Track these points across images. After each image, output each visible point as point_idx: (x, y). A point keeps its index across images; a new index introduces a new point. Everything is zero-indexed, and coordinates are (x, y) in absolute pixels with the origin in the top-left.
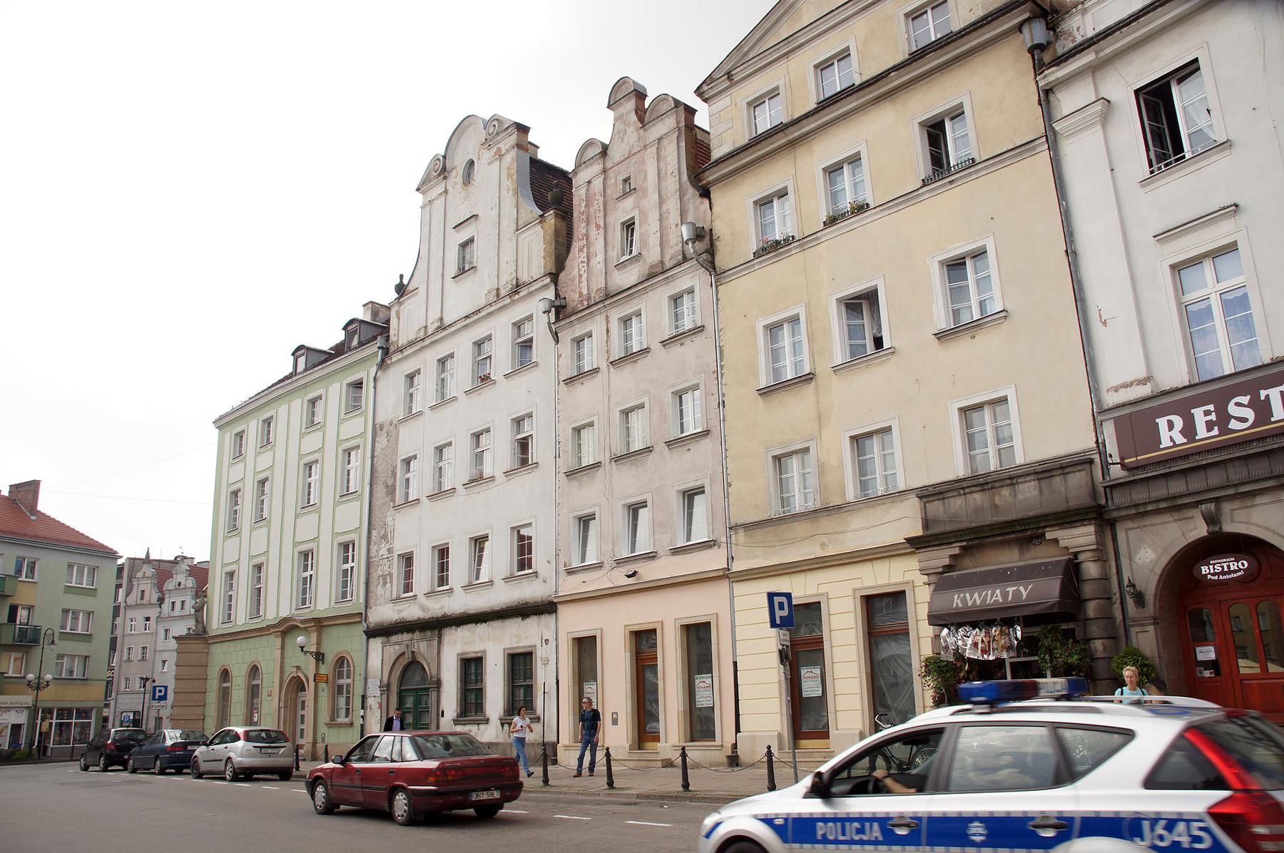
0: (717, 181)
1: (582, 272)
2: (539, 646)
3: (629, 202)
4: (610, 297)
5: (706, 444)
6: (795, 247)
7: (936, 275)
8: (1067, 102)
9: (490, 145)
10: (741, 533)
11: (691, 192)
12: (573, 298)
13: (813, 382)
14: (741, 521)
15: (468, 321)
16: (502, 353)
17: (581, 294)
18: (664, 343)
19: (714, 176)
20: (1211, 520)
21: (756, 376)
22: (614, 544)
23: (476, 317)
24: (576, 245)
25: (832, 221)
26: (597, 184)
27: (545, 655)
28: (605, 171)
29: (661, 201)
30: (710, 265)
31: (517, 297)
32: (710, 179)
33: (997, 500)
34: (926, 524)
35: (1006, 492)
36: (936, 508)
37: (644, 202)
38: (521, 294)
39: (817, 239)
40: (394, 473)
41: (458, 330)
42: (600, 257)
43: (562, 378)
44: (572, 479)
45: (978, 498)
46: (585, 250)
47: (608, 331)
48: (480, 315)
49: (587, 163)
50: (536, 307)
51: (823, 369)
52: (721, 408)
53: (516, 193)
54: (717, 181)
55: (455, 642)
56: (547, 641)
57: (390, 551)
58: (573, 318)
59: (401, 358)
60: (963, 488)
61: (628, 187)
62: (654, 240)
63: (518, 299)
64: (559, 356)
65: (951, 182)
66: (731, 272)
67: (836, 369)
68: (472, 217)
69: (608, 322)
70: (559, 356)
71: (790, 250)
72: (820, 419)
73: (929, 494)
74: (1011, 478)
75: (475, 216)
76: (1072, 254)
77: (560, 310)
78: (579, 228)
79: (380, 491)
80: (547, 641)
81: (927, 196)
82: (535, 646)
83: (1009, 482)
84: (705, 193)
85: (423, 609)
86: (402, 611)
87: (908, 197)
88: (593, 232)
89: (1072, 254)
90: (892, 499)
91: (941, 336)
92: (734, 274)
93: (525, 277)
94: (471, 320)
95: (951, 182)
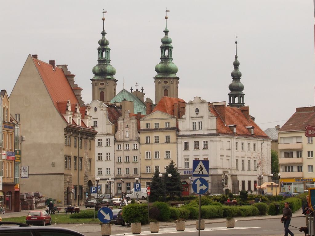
3: (127, 129)
4: (124, 141)
7: (165, 153)
8: (179, 140)
11: (137, 131)
12: (117, 139)
16: (104, 142)
18: (133, 150)
20: (184, 180)
21: (145, 157)
24: (118, 131)
26: (122, 124)
28: (123, 122)
29: (133, 131)
30: (139, 143)
37: (130, 130)
50: (112, 138)
53: (106, 118)
61: (128, 127)
62: (131, 136)
67: (154, 159)
72: (152, 164)
75: (97, 118)
76: (177, 154)
77: (115, 140)
78: (119, 129)
84: (139, 132)
87: (163, 143)
88: (121, 130)
89: (177, 154)
91: (165, 159)
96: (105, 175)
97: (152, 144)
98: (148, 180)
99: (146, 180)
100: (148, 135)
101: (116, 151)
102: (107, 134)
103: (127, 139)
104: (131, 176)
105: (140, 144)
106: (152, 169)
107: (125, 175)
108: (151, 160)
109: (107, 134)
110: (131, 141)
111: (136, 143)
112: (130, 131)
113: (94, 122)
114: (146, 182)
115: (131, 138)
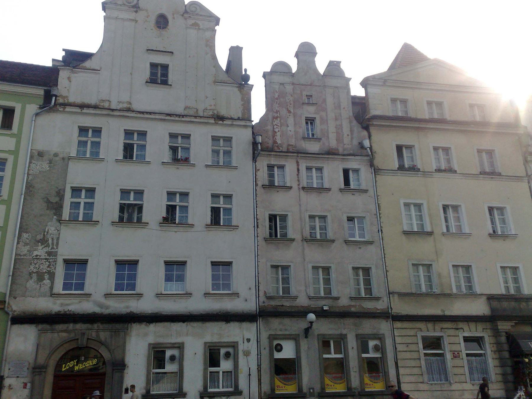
0: (377, 125)
1: (277, 130)
2: (240, 342)
3: (312, 109)
5: (372, 248)
6: (420, 174)
9: (190, 17)
10: (396, 296)
13: (433, 235)
14: (397, 290)
15: (168, 118)
17: (275, 142)
19: (377, 123)
21: (401, 224)
22: (306, 287)
23: (177, 119)
25: (439, 170)
27: (246, 348)
31: (221, 122)
32: (375, 123)
33: (522, 306)
34: (492, 310)
35: (524, 304)
36: (495, 304)
38: (225, 122)
39: (432, 175)
40: (60, 195)
41: (155, 119)
42: (291, 128)
43: (260, 183)
44: (269, 243)
45: (513, 304)
46: (279, 119)
47: (298, 170)
48: (183, 119)
49: (282, 74)
51: (437, 231)
52: (380, 233)
54: (377, 125)
55: (146, 335)
56: (249, 340)
57: (52, 254)
58: (273, 153)
59: (79, 112)
60: (508, 299)
63: (220, 124)
64: (256, 170)
65: (492, 178)
66: (385, 171)
68: (171, 52)
69: (298, 165)
70: (256, 170)
71: (418, 174)
73: (491, 298)
74: (527, 299)
75: (172, 53)
79: (38, 205)
80: (249, 340)
81: (481, 179)
82: (237, 343)
83: (526, 300)
84: (366, 128)
85: (101, 306)
86: (67, 305)
90: (475, 296)
92: (386, 173)
93: (223, 112)
94: (172, 118)
95: (492, 178)
96: (207, 295)
97: (426, 174)
98: (430, 325)
99: (421, 325)
100: (405, 138)
101: (259, 189)
102: (219, 118)
103: (313, 147)
104: (344, 302)
105: (377, 171)
106: (439, 275)
107: (310, 298)
108: (431, 239)
109: (219, 118)
110: (331, 153)
111: (352, 164)
112: (322, 119)
113: (153, 66)
114: (420, 335)
115: (333, 143)
